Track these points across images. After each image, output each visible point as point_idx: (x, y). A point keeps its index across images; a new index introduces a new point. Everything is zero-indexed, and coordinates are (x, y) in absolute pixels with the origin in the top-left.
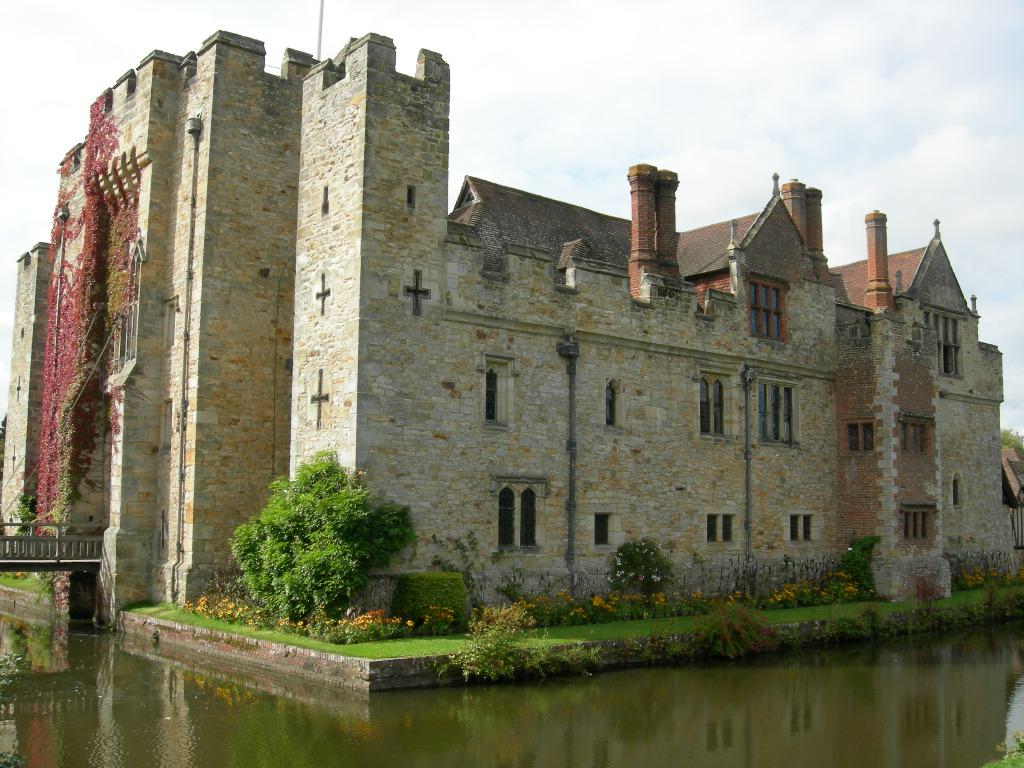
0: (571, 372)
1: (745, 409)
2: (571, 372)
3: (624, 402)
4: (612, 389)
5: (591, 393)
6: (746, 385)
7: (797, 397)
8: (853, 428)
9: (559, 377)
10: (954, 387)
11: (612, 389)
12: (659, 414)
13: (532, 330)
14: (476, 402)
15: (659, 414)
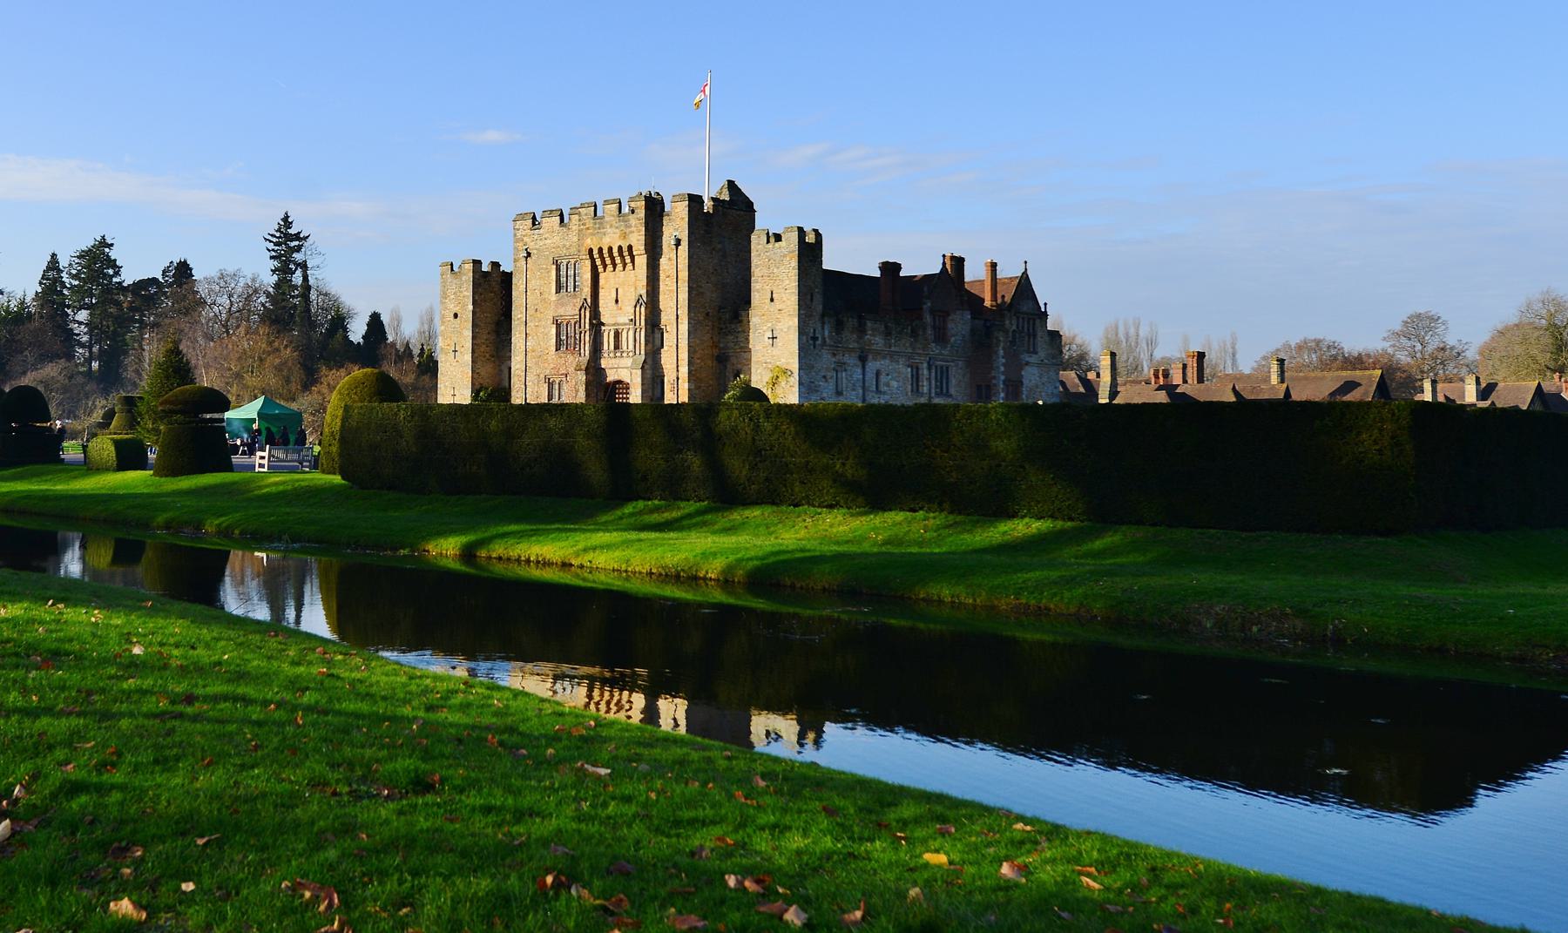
0: (864, 368)
1: (929, 379)
2: (864, 368)
3: (883, 379)
4: (878, 374)
5: (870, 376)
6: (929, 368)
7: (952, 371)
8: (979, 387)
9: (859, 370)
10: (1033, 359)
11: (878, 374)
12: (894, 384)
13: (851, 350)
14: (832, 385)
15: (894, 384)
